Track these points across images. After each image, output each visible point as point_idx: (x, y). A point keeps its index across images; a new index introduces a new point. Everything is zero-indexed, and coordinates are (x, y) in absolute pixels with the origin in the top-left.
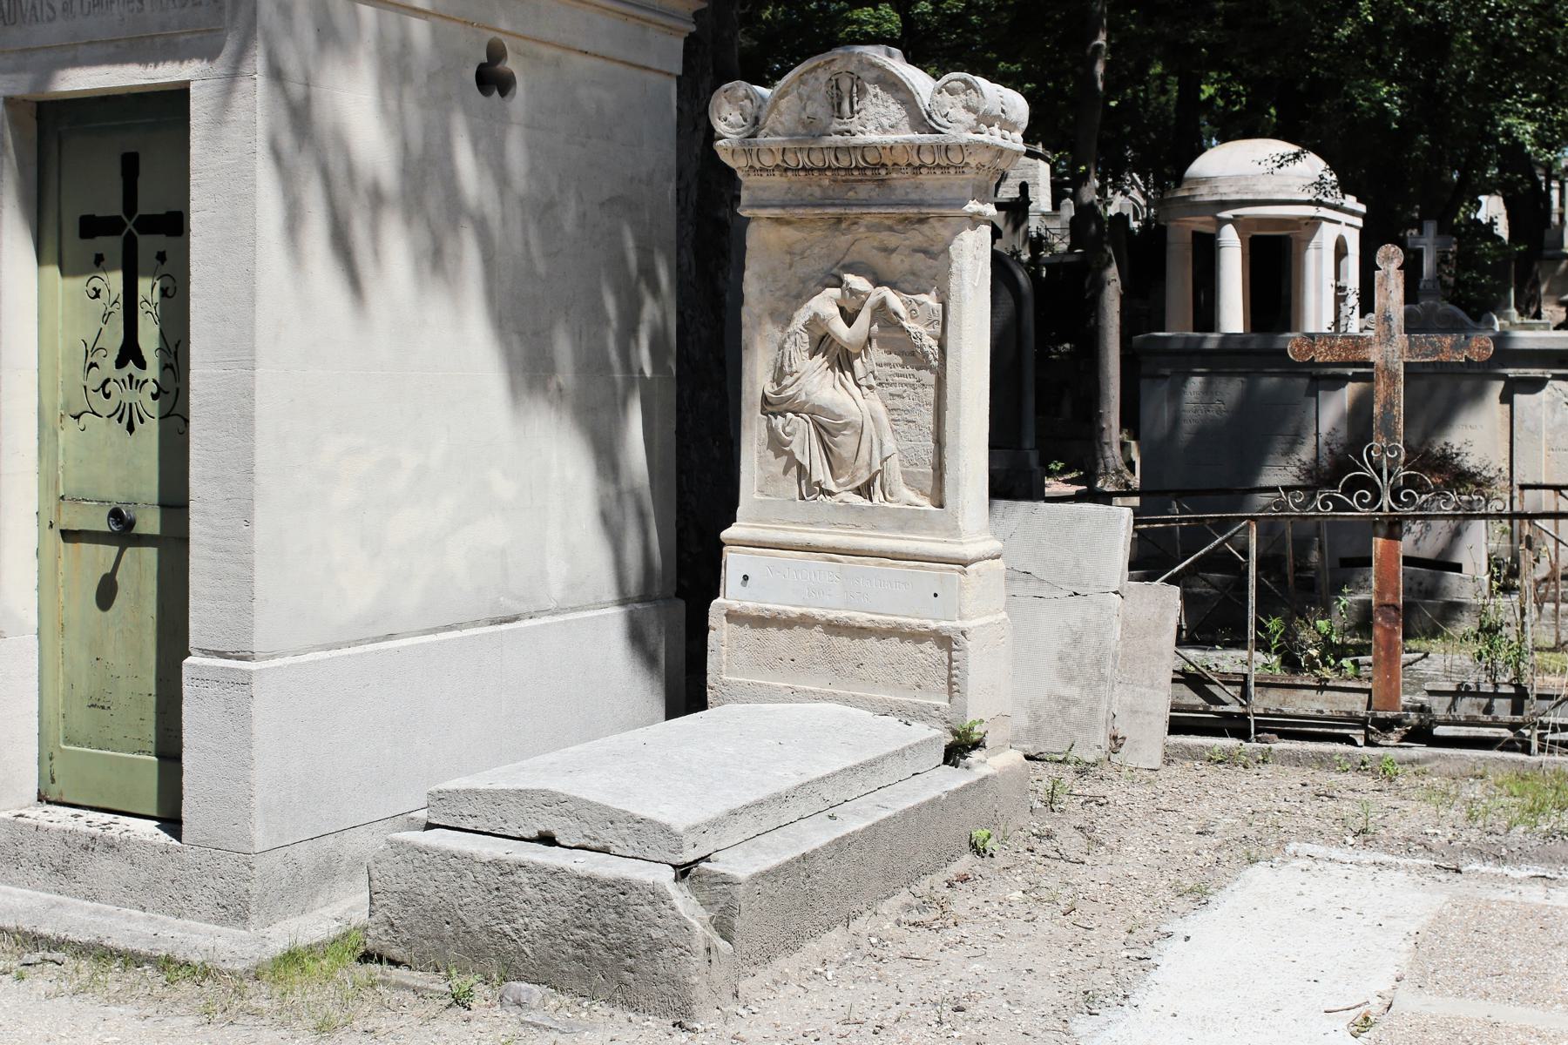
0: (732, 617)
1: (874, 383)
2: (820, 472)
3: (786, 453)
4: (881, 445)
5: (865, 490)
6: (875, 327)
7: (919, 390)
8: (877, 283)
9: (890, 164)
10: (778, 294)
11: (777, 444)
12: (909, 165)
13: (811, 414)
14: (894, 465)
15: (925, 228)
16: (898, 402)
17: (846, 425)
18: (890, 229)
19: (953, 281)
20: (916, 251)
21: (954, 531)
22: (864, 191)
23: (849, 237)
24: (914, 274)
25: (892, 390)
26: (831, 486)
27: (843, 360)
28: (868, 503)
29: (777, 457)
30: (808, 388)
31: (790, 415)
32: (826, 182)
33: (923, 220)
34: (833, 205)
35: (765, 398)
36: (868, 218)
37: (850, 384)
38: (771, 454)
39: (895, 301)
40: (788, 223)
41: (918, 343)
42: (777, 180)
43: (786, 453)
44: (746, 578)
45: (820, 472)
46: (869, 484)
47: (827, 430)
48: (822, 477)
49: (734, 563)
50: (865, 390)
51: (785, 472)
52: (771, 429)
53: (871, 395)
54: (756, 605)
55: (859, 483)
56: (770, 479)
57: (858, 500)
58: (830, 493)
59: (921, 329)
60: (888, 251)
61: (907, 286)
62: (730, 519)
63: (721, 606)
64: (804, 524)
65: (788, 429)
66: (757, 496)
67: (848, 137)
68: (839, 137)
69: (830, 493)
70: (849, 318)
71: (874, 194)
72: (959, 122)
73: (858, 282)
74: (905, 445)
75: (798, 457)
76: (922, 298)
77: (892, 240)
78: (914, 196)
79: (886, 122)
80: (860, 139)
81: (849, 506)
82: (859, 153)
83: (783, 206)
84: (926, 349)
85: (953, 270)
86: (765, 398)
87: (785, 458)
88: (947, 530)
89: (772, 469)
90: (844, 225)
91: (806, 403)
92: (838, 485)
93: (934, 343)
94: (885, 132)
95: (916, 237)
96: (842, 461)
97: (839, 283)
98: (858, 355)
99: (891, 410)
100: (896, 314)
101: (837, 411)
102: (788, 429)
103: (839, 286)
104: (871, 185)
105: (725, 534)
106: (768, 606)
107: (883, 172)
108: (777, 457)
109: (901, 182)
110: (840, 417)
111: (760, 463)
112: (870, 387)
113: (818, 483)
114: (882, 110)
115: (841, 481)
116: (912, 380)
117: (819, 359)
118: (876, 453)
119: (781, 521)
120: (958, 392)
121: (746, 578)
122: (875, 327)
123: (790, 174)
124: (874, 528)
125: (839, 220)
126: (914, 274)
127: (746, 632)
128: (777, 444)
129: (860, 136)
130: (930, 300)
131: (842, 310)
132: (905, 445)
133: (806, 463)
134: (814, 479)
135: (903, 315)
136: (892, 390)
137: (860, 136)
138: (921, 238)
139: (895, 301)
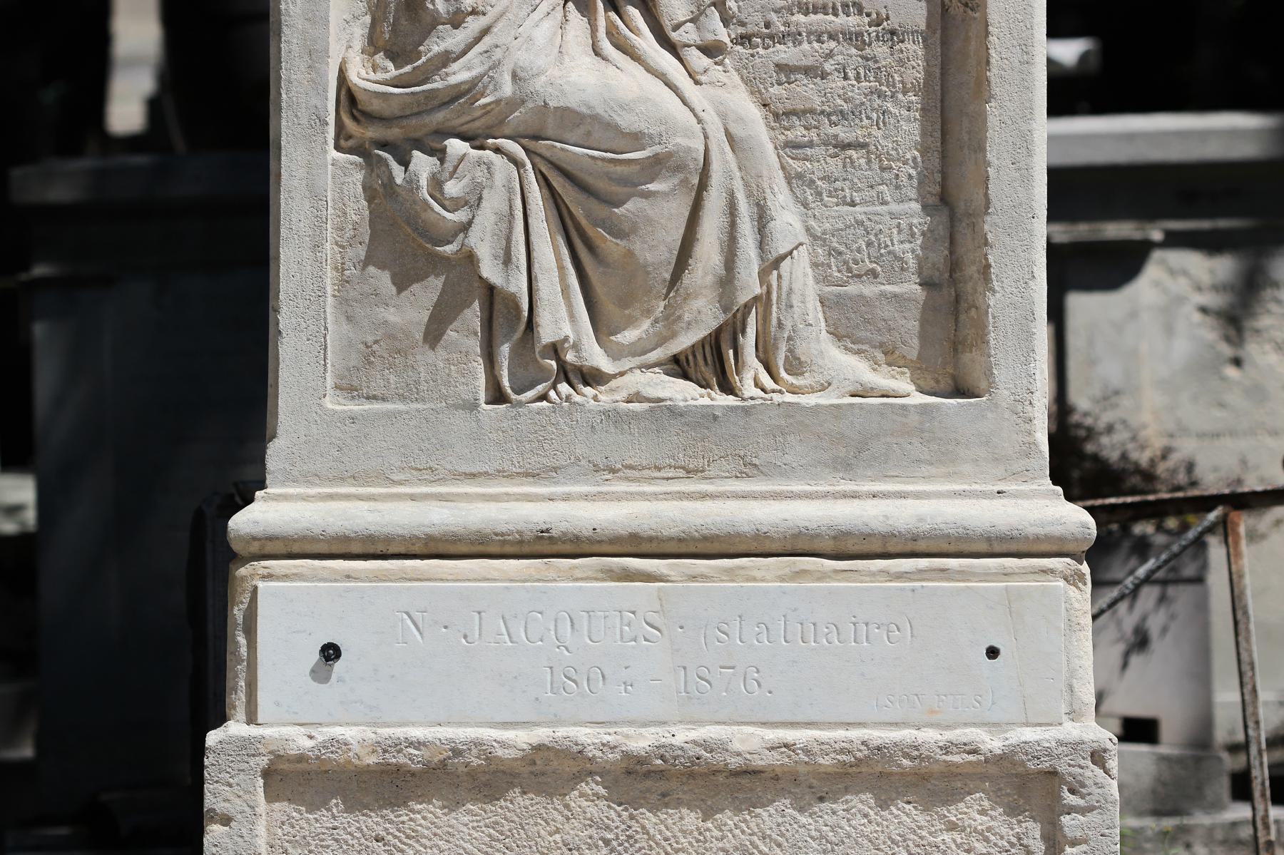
0: (292, 778)
1: (723, 35)
2: (563, 318)
3: (438, 264)
11: (404, 240)
13: (530, 137)
17: (657, 166)
25: (785, 53)
28: (730, 400)
29: (402, 283)
31: (456, 146)
35: (349, 98)
37: (646, 42)
43: (438, 264)
44: (331, 652)
47: (584, 186)
48: (567, 330)
49: (282, 615)
50: (698, 60)
52: (382, 195)
53: (716, 72)
54: (369, 734)
63: (246, 747)
64: (504, 475)
65: (452, 188)
74: (833, 215)
75: (490, 270)
81: (663, 411)
86: (349, 98)
89: (392, 316)
91: (514, 103)
96: (632, 269)
101: (626, 121)
102: (452, 188)
106: (417, 733)
108: (402, 283)
110: (637, 139)
111: (343, 301)
112: (711, 50)
113: (555, 350)
119: (431, 474)
121: (331, 652)
127: (333, 822)
132: (833, 215)
134: (547, 333)
136: (785, 53)
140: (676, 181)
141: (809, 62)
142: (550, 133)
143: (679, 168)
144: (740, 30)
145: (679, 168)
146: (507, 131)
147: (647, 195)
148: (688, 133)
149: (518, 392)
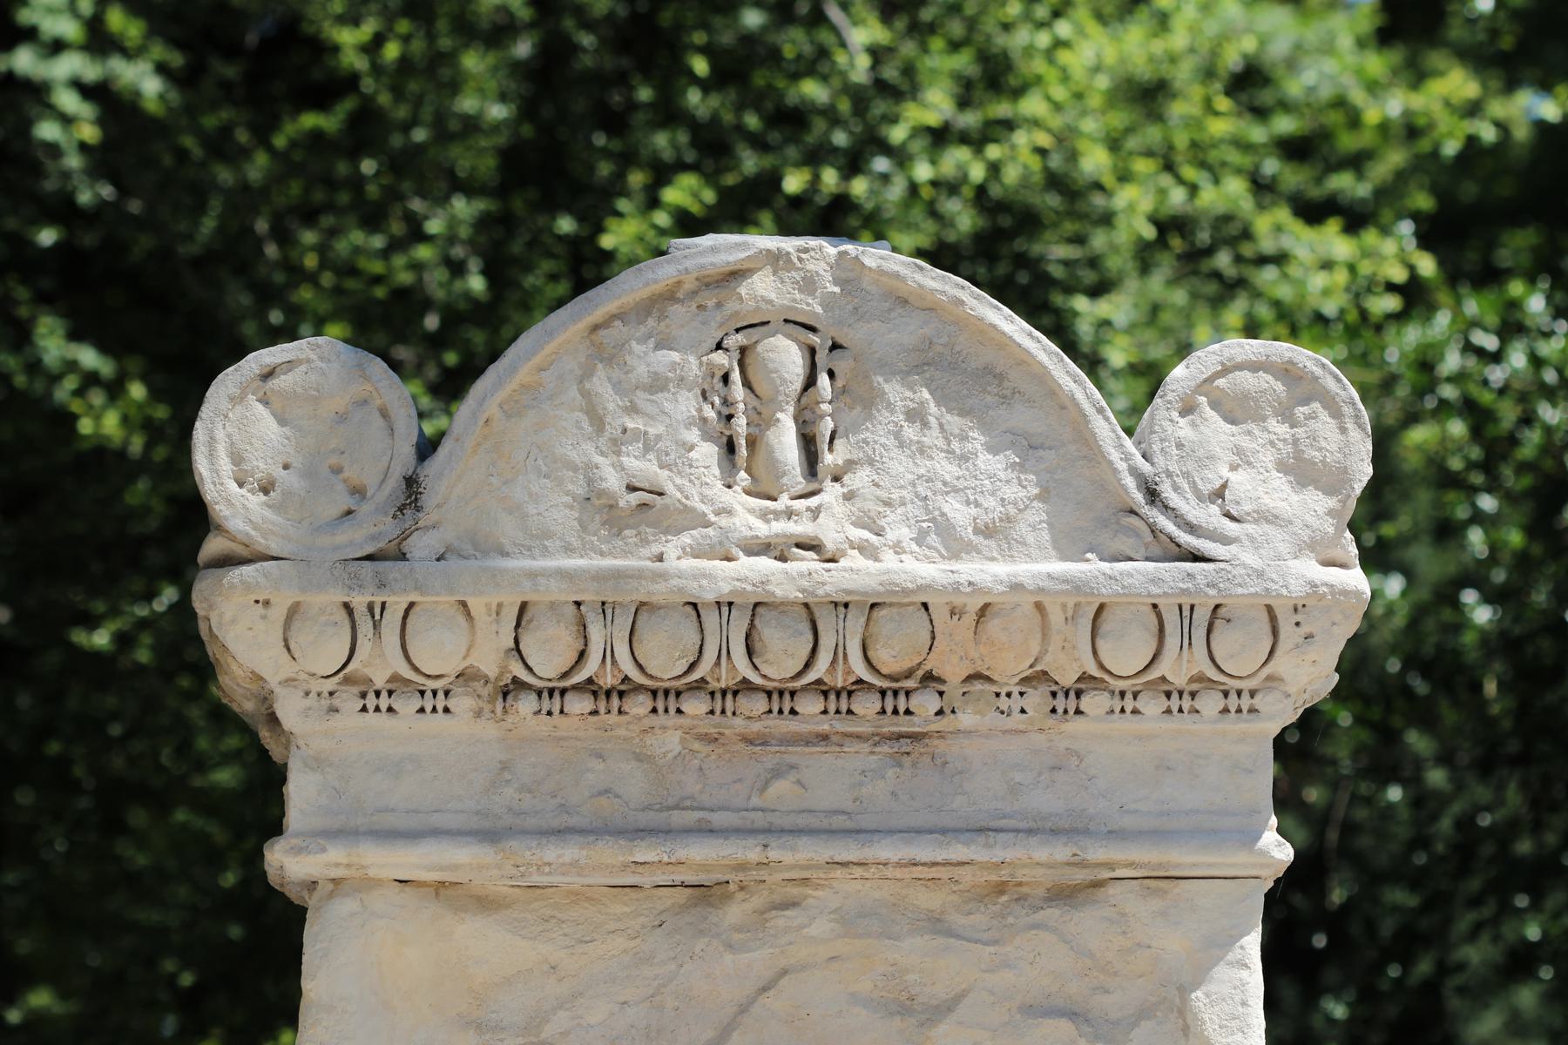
15: (1086, 923)
18: (936, 924)
22: (830, 779)
23: (759, 960)
33: (1064, 895)
36: (847, 887)
40: (485, 904)
67: (807, 563)
68: (765, 564)
72: (1267, 517)
77: (935, 966)
78: (1044, 801)
79: (958, 512)
80: (856, 573)
90: (735, 912)
94: (955, 547)
95: (1043, 956)
109: (988, 744)
114: (948, 470)
125: (707, 893)
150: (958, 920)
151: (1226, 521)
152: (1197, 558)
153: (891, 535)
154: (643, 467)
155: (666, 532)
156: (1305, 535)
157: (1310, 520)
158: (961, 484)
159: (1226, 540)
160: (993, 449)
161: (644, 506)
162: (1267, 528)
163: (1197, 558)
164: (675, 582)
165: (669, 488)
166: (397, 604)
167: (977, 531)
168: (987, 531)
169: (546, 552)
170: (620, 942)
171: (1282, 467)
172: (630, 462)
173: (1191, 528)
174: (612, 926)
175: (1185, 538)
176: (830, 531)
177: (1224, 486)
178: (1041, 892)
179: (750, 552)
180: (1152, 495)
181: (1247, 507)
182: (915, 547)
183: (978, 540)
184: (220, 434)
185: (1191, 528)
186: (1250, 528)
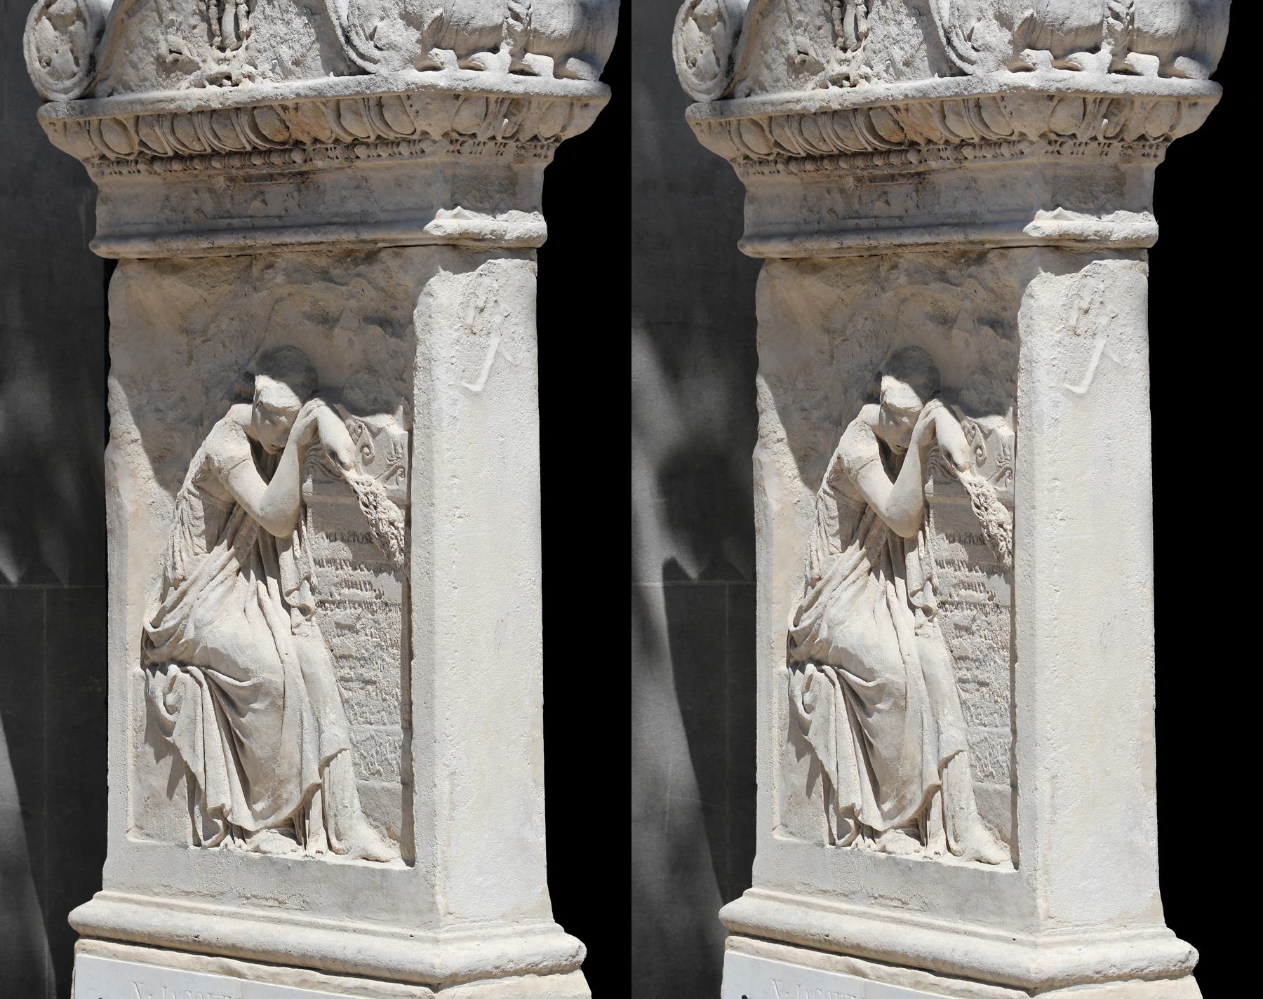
1: (311, 601)
2: (224, 789)
4: (320, 731)
5: (295, 829)
6: (309, 483)
7: (380, 616)
8: (307, 392)
9: (306, 139)
10: (171, 416)
12: (337, 141)
14: (344, 774)
15: (375, 271)
16: (349, 643)
18: (325, 276)
19: (419, 381)
20: (369, 320)
21: (426, 915)
24: (370, 369)
25: (340, 615)
26: (243, 818)
27: (261, 558)
30: (200, 612)
32: (220, 182)
33: (371, 257)
34: (231, 230)
38: (150, 750)
39: (336, 431)
41: (373, 516)
42: (144, 180)
45: (224, 789)
46: (303, 812)
51: (171, 790)
53: (306, 627)
55: (287, 812)
56: (150, 805)
57: (283, 847)
58: (244, 834)
59: (378, 486)
60: (327, 320)
61: (356, 396)
62: (90, 885)
66: (133, 838)
69: (244, 834)
70: (266, 463)
71: (291, 204)
72: (392, 47)
73: (273, 391)
76: (380, 420)
77: (329, 298)
79: (286, 53)
80: (248, 90)
82: (244, 119)
83: (153, 236)
84: (385, 528)
85: (419, 360)
87: (169, 760)
88: (418, 912)
92: (257, 816)
93: (397, 514)
94: (287, 74)
97: (247, 396)
98: (288, 543)
99: (340, 658)
100: (334, 454)
103: (248, 400)
104: (287, 186)
105: (80, 914)
107: (297, 157)
110: (245, 674)
111: (138, 769)
112: (304, 610)
113: (220, 812)
115: (259, 806)
116: (368, 595)
117: (222, 552)
118: (310, 748)
120: (430, 619)
122: (309, 483)
123: (158, 167)
124: (306, 906)
126: (370, 369)
128: (158, 732)
129: (246, 85)
130: (392, 425)
131: (257, 449)
133: (198, 769)
135: (345, 456)
136: (340, 615)
137: (246, 85)
138: (371, 292)
139: (336, 431)
140: (267, 703)
141: (348, 622)
142: (213, 665)
143: (267, 694)
144: (320, 598)
145: (267, 694)
146: (197, 662)
147: (254, 711)
148: (271, 670)
149: (205, 839)
150: (337, 272)
151: (376, 51)
152: (364, 72)
153: (260, 69)
154: (176, 40)
155: (186, 73)
156: (407, 55)
157: (409, 46)
158: (287, 37)
159: (375, 62)
160: (298, 14)
161: (176, 61)
162: (393, 52)
163: (364, 72)
164: (178, 103)
165: (186, 51)
166: (94, 119)
167: (293, 63)
168: (296, 63)
169: (147, 89)
170: (225, 288)
171: (402, 17)
172: (171, 38)
173: (362, 56)
174: (223, 278)
175: (360, 62)
176: (234, 70)
177: (375, 30)
178: (363, 255)
179: (212, 82)
180: (348, 40)
181: (384, 42)
182: (271, 74)
183: (294, 68)
184: (32, 38)
185: (362, 56)
186: (385, 53)
